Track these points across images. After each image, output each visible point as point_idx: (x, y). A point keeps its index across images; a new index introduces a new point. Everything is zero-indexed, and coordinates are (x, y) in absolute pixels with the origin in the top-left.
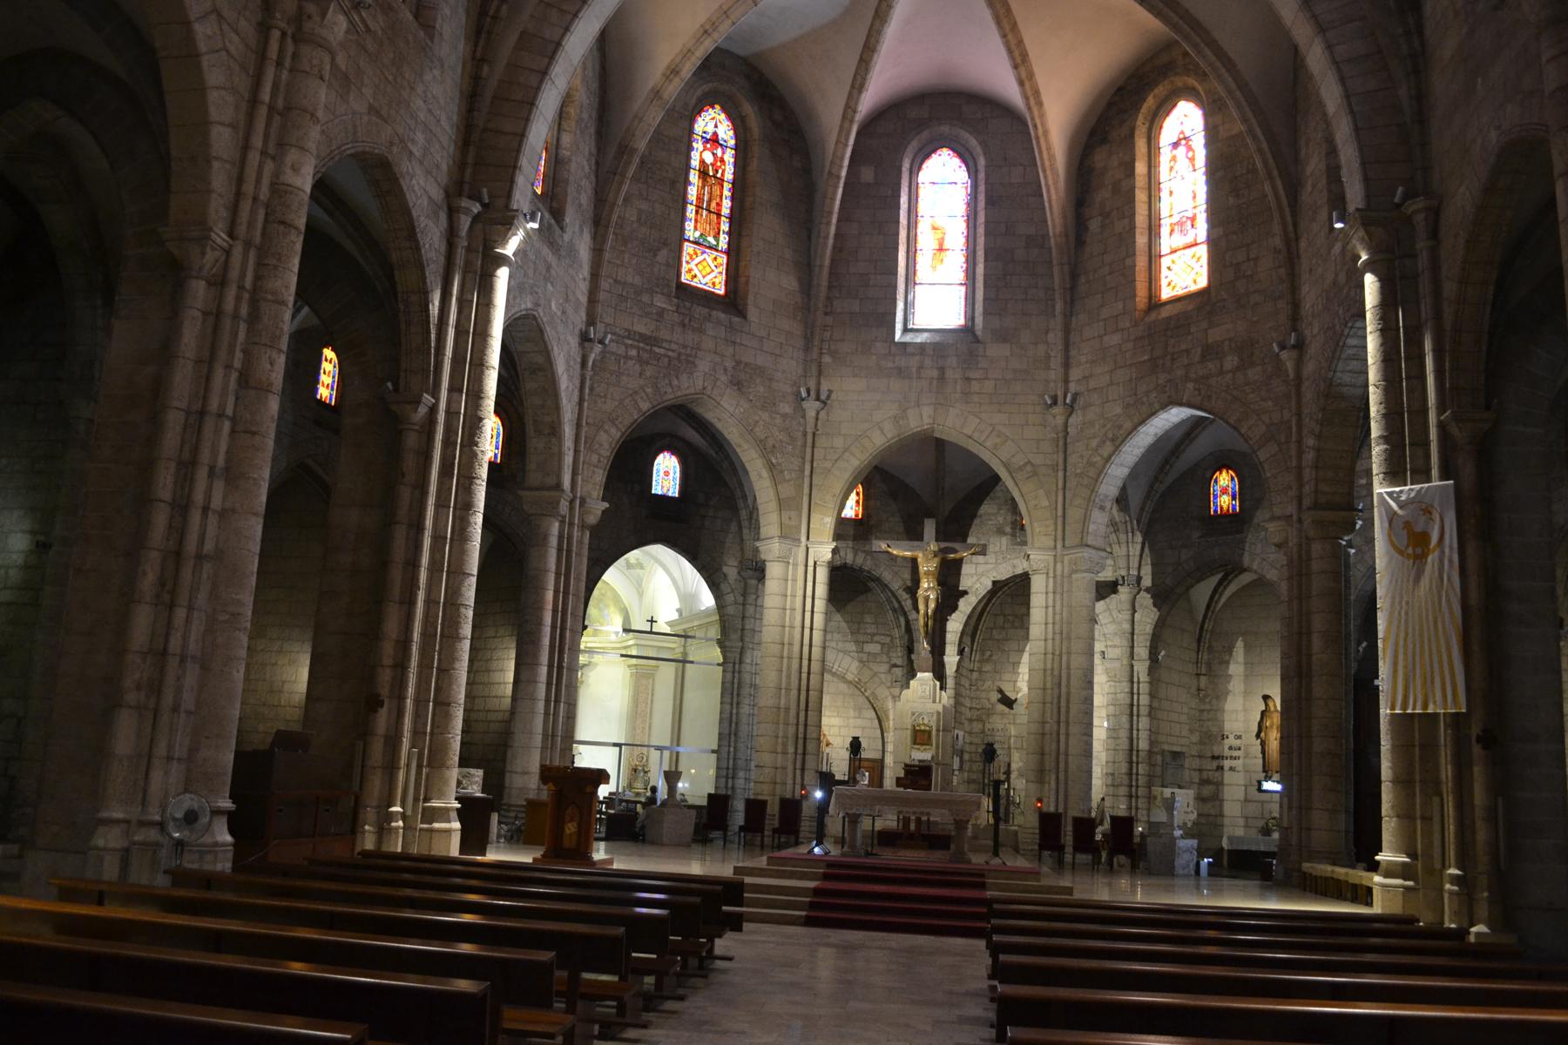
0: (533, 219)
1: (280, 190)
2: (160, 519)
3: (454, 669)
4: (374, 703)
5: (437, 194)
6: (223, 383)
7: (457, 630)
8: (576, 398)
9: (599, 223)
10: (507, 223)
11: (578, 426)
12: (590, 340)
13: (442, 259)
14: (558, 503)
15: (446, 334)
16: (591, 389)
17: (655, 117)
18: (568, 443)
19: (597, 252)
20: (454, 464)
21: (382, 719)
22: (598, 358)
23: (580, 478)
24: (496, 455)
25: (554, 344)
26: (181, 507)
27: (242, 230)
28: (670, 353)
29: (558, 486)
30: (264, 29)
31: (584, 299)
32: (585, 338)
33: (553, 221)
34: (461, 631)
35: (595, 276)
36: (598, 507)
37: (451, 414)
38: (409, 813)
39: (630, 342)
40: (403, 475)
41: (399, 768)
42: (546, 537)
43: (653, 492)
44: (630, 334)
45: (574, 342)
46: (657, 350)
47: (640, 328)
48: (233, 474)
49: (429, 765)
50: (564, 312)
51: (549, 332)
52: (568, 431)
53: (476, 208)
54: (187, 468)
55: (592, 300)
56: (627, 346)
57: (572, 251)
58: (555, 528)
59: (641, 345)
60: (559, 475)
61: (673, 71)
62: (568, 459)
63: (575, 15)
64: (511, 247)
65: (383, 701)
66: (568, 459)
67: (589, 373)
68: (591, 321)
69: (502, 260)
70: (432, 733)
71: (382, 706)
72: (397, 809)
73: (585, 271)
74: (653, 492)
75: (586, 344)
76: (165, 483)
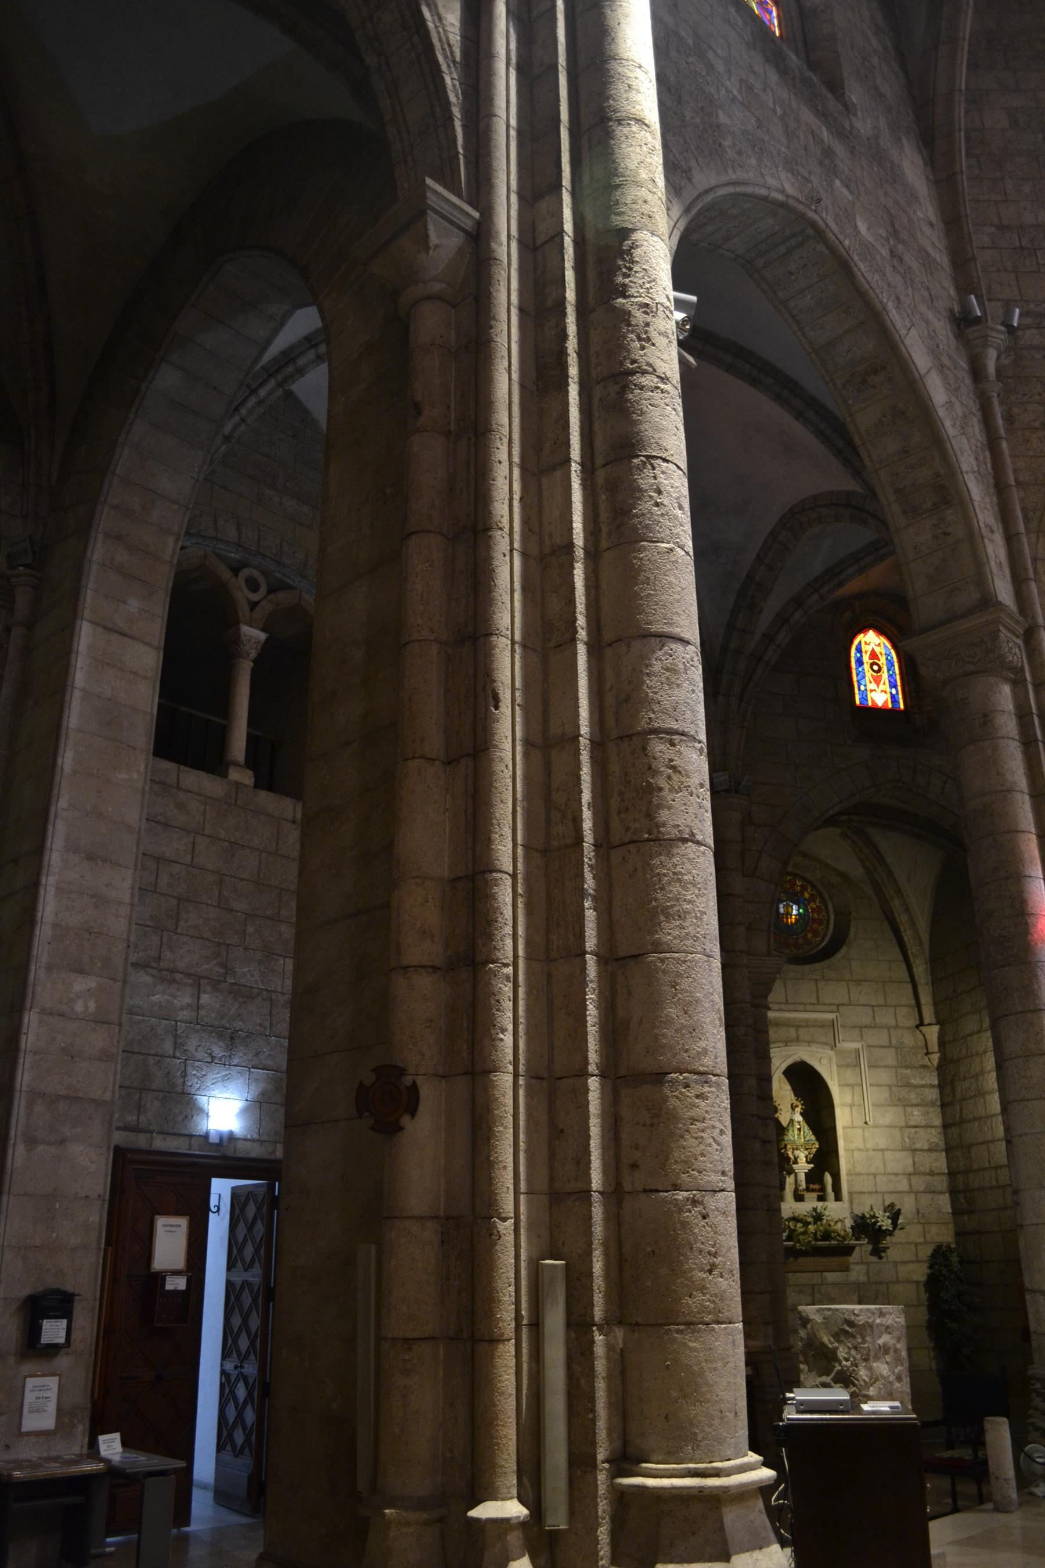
3: (658, 947)
7: (649, 815)
11: (1000, 489)
14: (995, 635)
16: (1009, 419)
20: (563, 353)
22: (1005, 361)
23: (1033, 587)
24: (893, 698)
25: (890, 306)
29: (988, 602)
34: (664, 815)
38: (558, 1520)
40: (418, 409)
41: (495, 1341)
42: (987, 718)
49: (618, 1316)
58: (1004, 696)
60: (981, 580)
62: (995, 549)
65: (414, 1090)
66: (995, 549)
67: (994, 389)
68: (965, 285)
70: (615, 1194)
71: (412, 1108)
75: (971, 332)
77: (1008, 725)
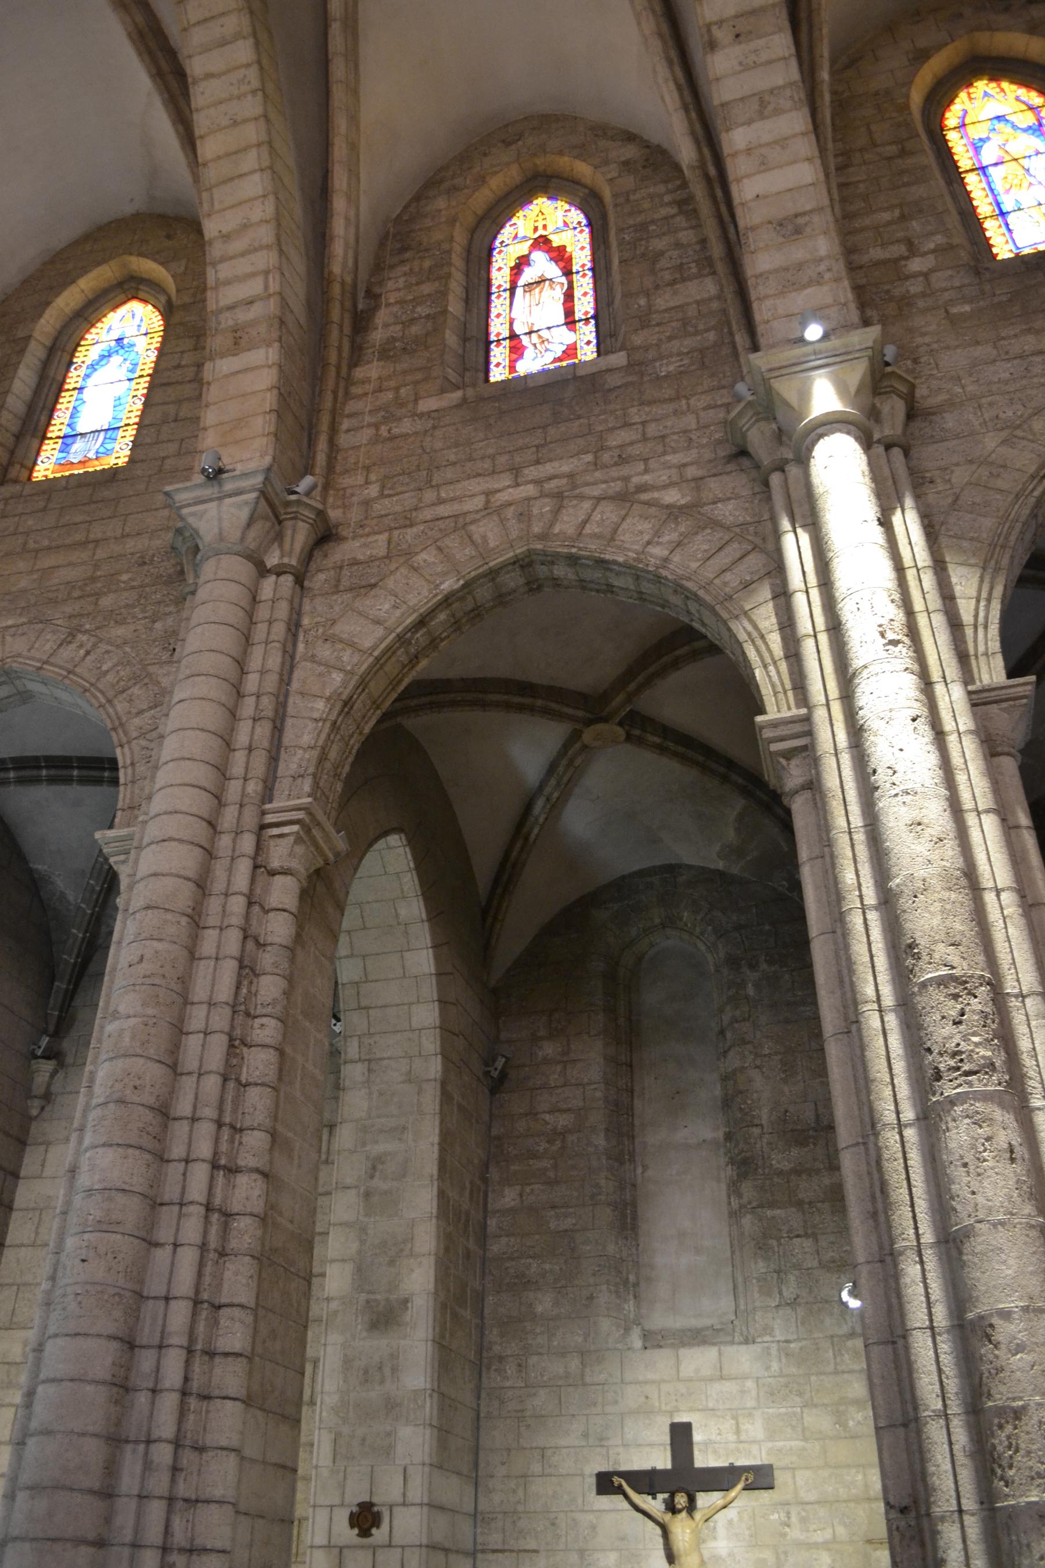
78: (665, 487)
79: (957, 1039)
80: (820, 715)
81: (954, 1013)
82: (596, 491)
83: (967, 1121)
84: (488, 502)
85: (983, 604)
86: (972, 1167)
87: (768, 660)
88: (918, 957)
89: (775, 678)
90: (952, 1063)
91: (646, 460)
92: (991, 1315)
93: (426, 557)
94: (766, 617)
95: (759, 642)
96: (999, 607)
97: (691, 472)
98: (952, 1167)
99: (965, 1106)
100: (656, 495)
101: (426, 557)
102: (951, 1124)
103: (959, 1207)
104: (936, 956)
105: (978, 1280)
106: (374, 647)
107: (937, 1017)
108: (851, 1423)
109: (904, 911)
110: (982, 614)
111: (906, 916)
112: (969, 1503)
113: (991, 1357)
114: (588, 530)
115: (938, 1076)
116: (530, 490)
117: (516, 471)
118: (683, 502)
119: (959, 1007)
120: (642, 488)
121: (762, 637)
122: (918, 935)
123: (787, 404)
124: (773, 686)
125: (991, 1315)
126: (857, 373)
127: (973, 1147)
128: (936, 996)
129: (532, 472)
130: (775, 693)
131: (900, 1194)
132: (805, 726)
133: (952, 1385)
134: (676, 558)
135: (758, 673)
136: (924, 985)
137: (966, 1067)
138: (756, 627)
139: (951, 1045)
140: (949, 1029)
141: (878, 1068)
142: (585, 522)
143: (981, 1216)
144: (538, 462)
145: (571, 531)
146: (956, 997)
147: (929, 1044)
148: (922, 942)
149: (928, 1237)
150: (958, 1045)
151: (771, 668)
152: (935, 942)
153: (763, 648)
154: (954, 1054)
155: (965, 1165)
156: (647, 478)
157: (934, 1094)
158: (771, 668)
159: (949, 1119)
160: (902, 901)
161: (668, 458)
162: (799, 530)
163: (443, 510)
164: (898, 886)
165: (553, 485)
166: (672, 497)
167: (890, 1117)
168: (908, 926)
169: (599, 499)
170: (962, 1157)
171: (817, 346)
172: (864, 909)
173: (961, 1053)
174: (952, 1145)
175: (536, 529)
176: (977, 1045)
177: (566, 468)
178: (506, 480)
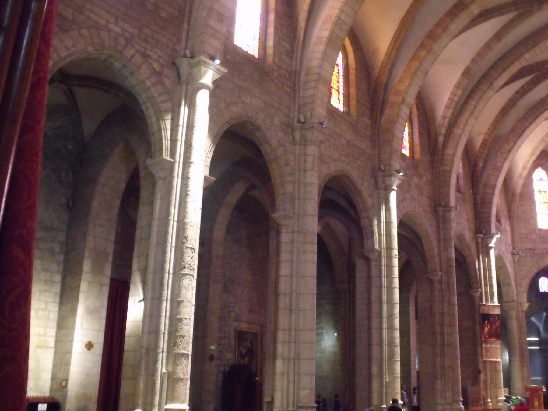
0: (497, 234)
1: (449, 259)
2: (439, 337)
4: (479, 372)
5: (472, 235)
6: (446, 304)
8: (513, 273)
9: (510, 217)
10: (492, 238)
12: (515, 254)
13: (476, 252)
15: (481, 271)
16: (518, 268)
17: (521, 182)
18: (514, 287)
19: (512, 226)
21: (482, 377)
26: (442, 334)
27: (443, 270)
28: (540, 252)
30: (438, 223)
31: (510, 242)
32: (513, 254)
33: (499, 225)
35: (512, 234)
36: (526, 306)
37: (486, 293)
39: (527, 252)
43: (541, 291)
44: (527, 249)
45: (510, 256)
46: (536, 252)
47: (529, 246)
48: (451, 325)
50: (506, 249)
51: (504, 257)
52: (513, 283)
53: (482, 236)
54: (442, 325)
55: (513, 241)
56: (526, 253)
57: (505, 230)
59: (530, 251)
61: (524, 168)
63: (498, 176)
64: (492, 244)
68: (514, 249)
69: (491, 248)
72: (489, 400)
73: (509, 234)
74: (541, 291)
75: (514, 256)
76: (438, 329)
77: (514, 318)
78: (155, 61)
79: (191, 262)
80: (177, 165)
81: (191, 256)
82: (138, 47)
83: (188, 279)
84: (107, 25)
85: (209, 151)
86: (187, 289)
87: (166, 139)
88: (188, 241)
89: (167, 145)
90: (188, 266)
91: (152, 46)
92: (183, 318)
93: (85, 32)
94: (168, 124)
95: (165, 131)
96: (212, 154)
97: (162, 61)
98: (182, 287)
99: (189, 276)
100: (152, 62)
101: (85, 32)
102: (185, 279)
103: (182, 296)
104: (192, 242)
105: (182, 311)
106: (65, 58)
107: (188, 255)
108: (39, 315)
109: (187, 229)
110: (208, 154)
111: (187, 230)
112: (165, 350)
113: (181, 326)
114: (133, 60)
115: (184, 268)
116: (119, 30)
117: (117, 18)
118: (157, 70)
119: (193, 255)
120: (149, 56)
121: (166, 130)
122: (189, 236)
123: (200, 72)
124: (166, 147)
125: (183, 318)
126: (217, 77)
127: (188, 285)
128: (189, 251)
129: (120, 22)
130: (166, 150)
131: (166, 288)
132: (172, 165)
133: (167, 328)
134: (153, 90)
135: (164, 141)
136: (187, 247)
137: (191, 268)
138: (166, 126)
139: (189, 263)
140: (189, 259)
141: (168, 259)
142: (132, 57)
143: (186, 299)
144: (123, 20)
145: (128, 57)
146: (193, 253)
147: (184, 260)
148: (190, 238)
149: (169, 298)
150: (190, 263)
151: (166, 141)
152: (192, 239)
153: (166, 134)
154: (189, 265)
155: (186, 288)
156: (151, 53)
157: (183, 271)
158: (166, 141)
159: (185, 278)
160: (187, 226)
161: (157, 50)
162: (186, 107)
163: (92, 16)
164: (187, 222)
165: (126, 34)
166: (156, 66)
167: (167, 271)
168: (187, 232)
169: (138, 51)
170: (185, 286)
171: (215, 64)
172: (174, 220)
173: (190, 265)
174: (184, 283)
175: (119, 48)
176: (193, 264)
177: (131, 30)
178: (112, 20)
